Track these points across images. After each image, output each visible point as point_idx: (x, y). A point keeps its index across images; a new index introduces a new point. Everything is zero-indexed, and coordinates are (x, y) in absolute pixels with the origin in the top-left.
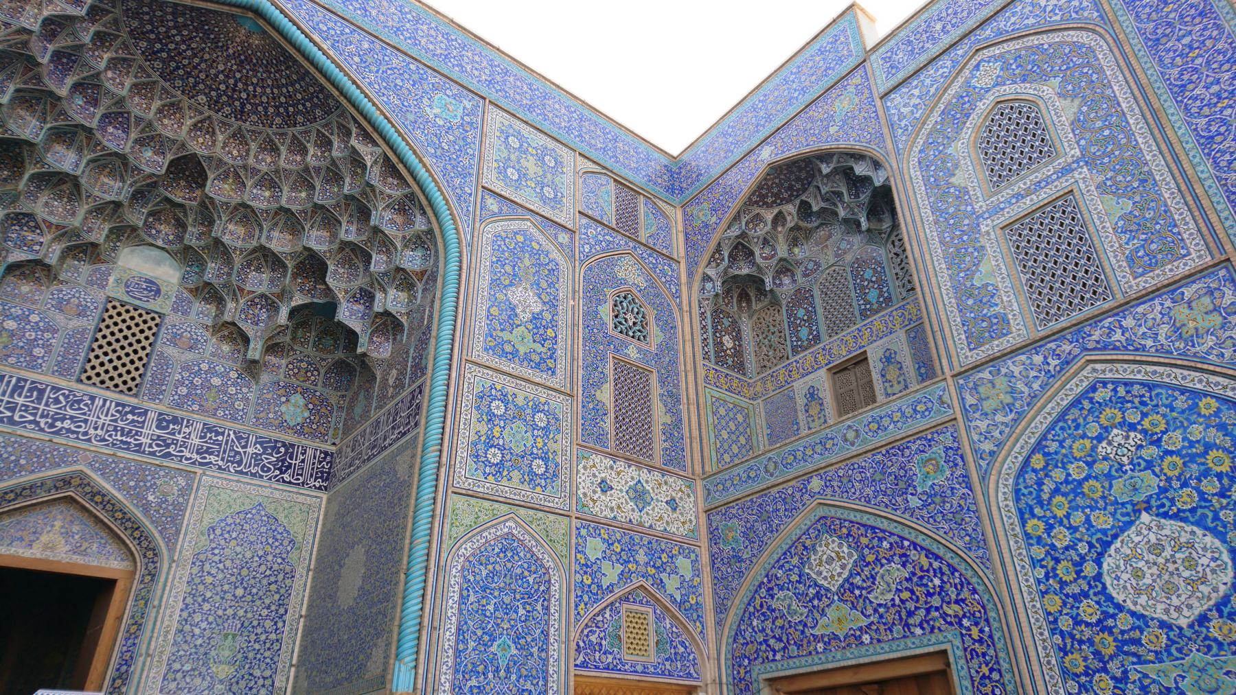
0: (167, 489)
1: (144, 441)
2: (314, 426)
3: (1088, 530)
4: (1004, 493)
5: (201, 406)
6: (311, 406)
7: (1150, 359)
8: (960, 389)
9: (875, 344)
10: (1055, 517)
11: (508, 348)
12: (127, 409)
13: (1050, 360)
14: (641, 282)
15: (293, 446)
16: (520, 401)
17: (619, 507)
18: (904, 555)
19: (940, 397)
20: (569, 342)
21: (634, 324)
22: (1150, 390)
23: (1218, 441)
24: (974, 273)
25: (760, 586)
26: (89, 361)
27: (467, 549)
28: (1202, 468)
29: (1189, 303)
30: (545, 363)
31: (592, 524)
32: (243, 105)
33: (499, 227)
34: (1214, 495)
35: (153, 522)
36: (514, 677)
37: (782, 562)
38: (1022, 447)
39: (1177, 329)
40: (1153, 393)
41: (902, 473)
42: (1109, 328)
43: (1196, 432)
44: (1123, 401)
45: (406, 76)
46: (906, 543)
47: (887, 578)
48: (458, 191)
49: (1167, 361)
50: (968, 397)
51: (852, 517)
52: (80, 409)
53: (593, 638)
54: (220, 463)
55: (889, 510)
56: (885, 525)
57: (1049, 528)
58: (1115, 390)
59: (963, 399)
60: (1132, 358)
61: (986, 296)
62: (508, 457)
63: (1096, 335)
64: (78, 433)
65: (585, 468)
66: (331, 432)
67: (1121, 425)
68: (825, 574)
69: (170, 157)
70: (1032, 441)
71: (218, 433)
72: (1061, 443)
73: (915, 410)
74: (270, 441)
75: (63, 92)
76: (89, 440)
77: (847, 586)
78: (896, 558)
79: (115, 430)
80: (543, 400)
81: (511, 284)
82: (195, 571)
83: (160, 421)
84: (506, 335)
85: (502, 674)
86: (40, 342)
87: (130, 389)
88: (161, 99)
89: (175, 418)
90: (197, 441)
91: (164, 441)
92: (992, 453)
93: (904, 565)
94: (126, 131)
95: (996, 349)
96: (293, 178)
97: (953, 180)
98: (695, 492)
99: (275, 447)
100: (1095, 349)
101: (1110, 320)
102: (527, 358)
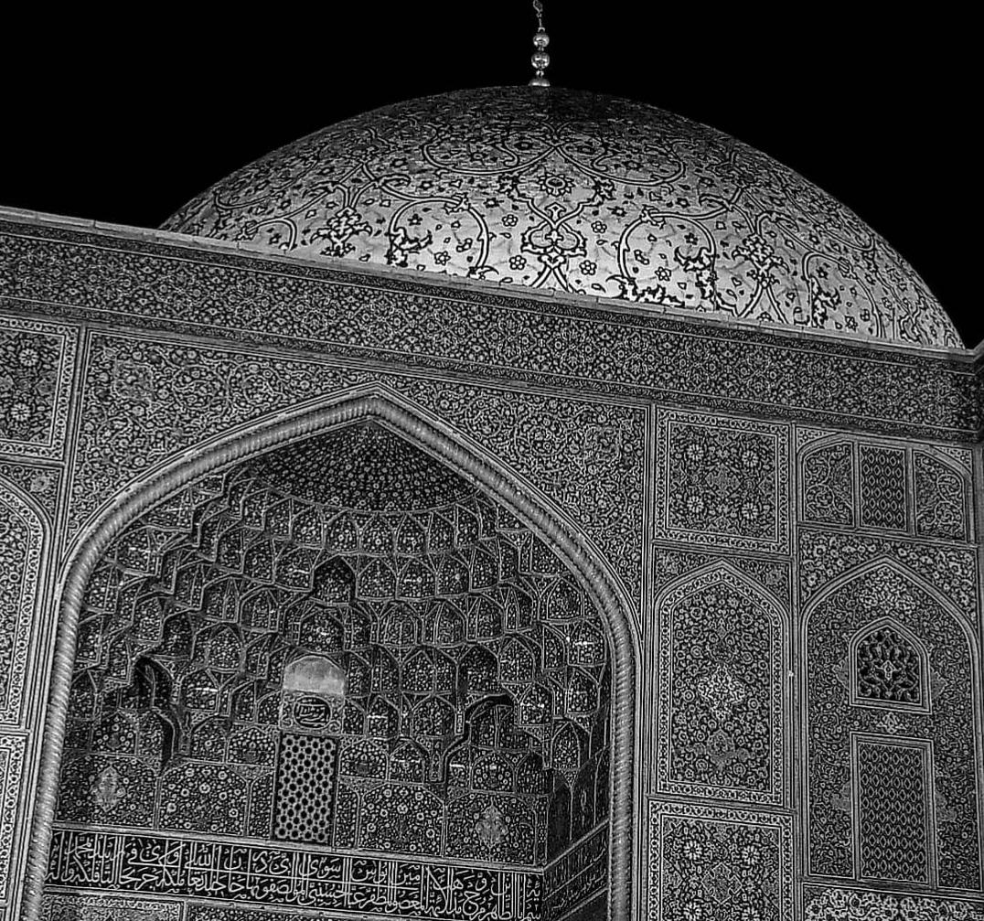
1: (345, 894)
5: (392, 842)
6: (508, 820)
12: (323, 861)
15: (494, 874)
20: (792, 736)
21: (895, 675)
26: (279, 812)
32: (377, 496)
45: (547, 422)
52: (281, 869)
54: (422, 907)
64: (283, 896)
65: (816, 910)
71: (414, 873)
74: (470, 874)
76: (295, 902)
79: (317, 887)
80: (752, 828)
83: (356, 868)
86: (233, 801)
87: (321, 837)
88: (295, 512)
89: (370, 862)
90: (393, 886)
91: (363, 891)
96: (443, 561)
99: (476, 879)
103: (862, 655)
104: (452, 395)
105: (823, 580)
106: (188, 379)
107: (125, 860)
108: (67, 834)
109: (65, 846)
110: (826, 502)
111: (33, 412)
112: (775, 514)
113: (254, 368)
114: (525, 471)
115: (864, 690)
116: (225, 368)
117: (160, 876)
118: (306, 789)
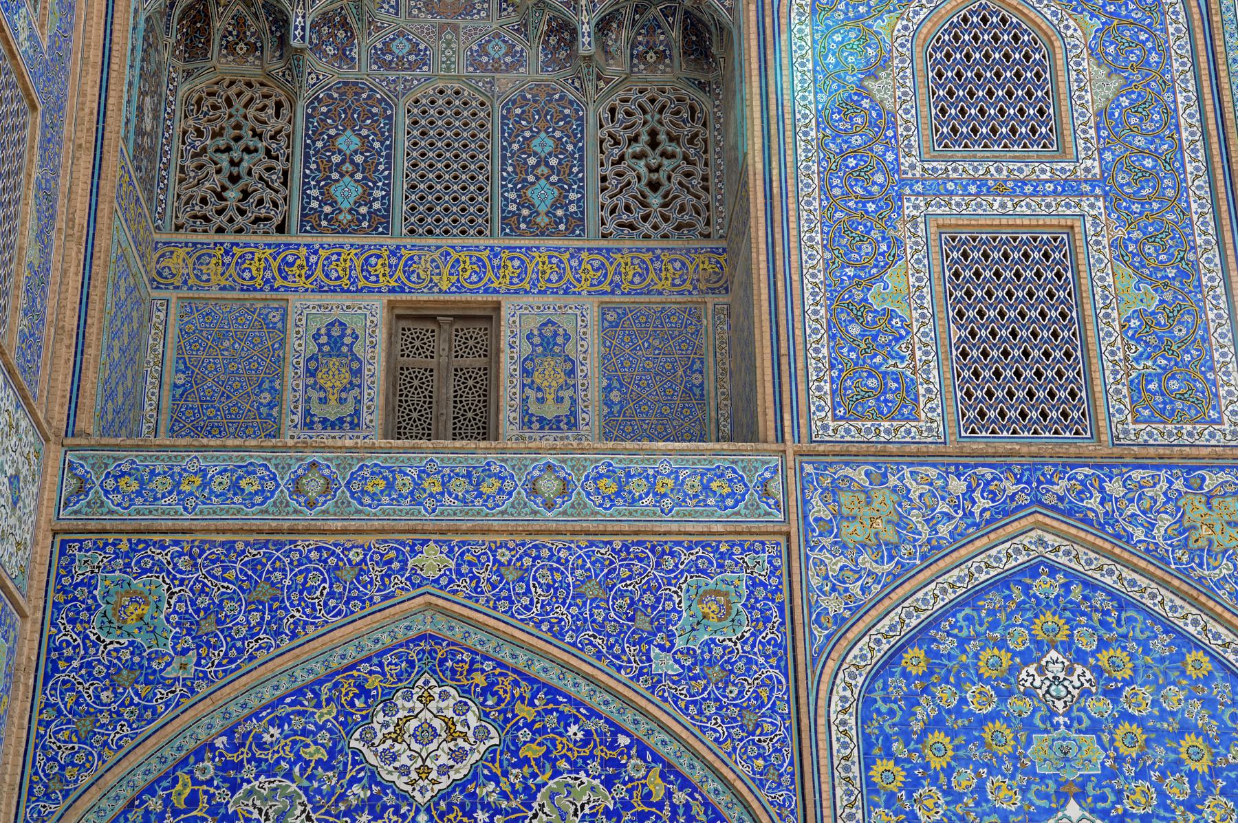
3: (977, 804)
4: (844, 699)
7: (1135, 560)
8: (805, 481)
9: (525, 300)
10: (926, 767)
13: (977, 495)
18: (614, 763)
19: (764, 483)
22: (1120, 608)
23: (1200, 723)
24: (872, 281)
25: (199, 754)
28: (1172, 756)
29: (1209, 497)
34: (1180, 803)
37: (282, 711)
38: (892, 628)
39: (1184, 529)
40: (1124, 615)
41: (649, 599)
42: (1082, 482)
43: (1174, 697)
44: (1076, 610)
46: (623, 740)
47: (563, 801)
49: (1159, 573)
50: (816, 501)
51: (505, 655)
55: (603, 664)
56: (583, 691)
57: (913, 784)
58: (1066, 587)
59: (805, 502)
60: (1108, 546)
61: (884, 333)
63: (1061, 487)
67: (1067, 646)
68: (404, 760)
70: (914, 622)
72: (962, 642)
73: (706, 487)
77: (457, 797)
78: (594, 766)
92: (839, 620)
93: (608, 783)
95: (884, 437)
97: (870, 84)
98: (43, 470)
100: (1053, 508)
101: (1087, 471)
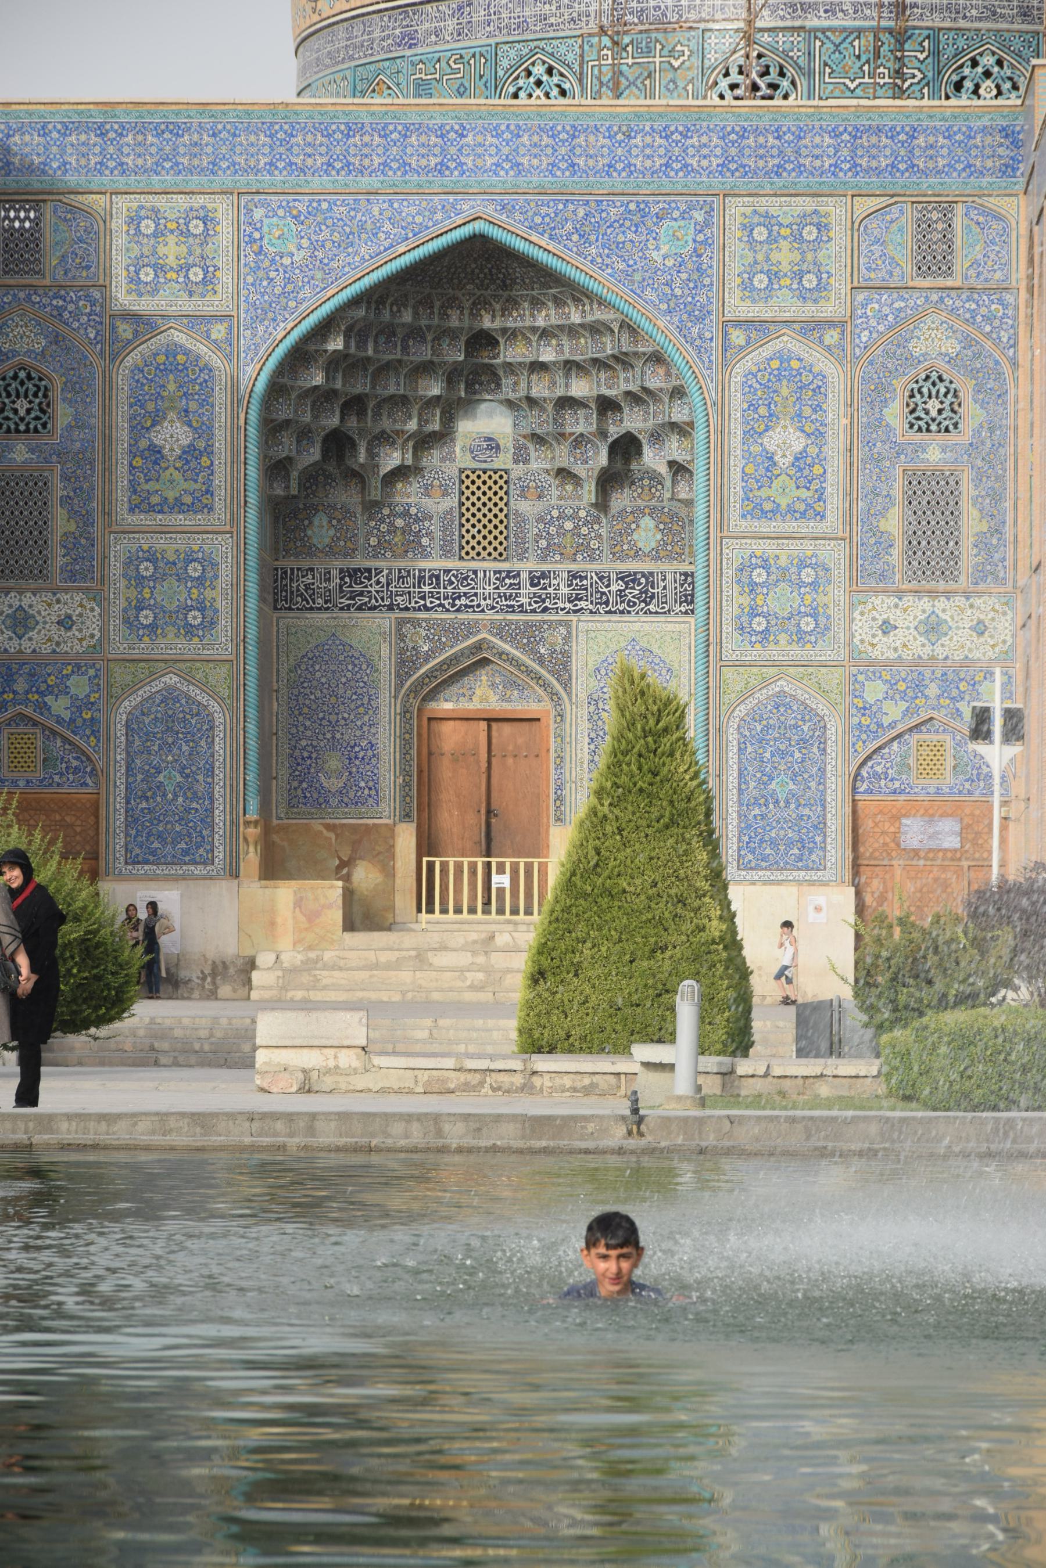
0: (551, 639)
1: (524, 600)
2: (669, 548)
5: (562, 554)
6: (661, 526)
11: (768, 506)
12: (504, 575)
14: (952, 347)
15: (651, 574)
16: (783, 562)
17: (905, 645)
21: (940, 411)
27: (742, 710)
30: (813, 511)
31: (871, 669)
32: (504, 282)
33: (748, 363)
35: (549, 672)
36: (793, 806)
45: (628, 223)
48: (698, 342)
53: (879, 769)
54: (590, 607)
62: (773, 623)
65: (862, 614)
66: (687, 550)
69: (464, 338)
71: (582, 578)
75: (370, 352)
80: (809, 553)
81: (766, 430)
82: (592, 708)
83: (532, 579)
84: (764, 493)
85: (782, 804)
87: (501, 555)
89: (543, 573)
90: (565, 590)
94: (424, 340)
102: (791, 510)
103: (912, 396)
104: (544, 210)
105: (875, 335)
106: (323, 227)
107: (341, 587)
108: (292, 570)
109: (291, 580)
110: (879, 262)
111: (206, 272)
112: (832, 281)
113: (376, 211)
114: (610, 271)
115: (912, 426)
116: (352, 213)
117: (370, 598)
118: (485, 516)
